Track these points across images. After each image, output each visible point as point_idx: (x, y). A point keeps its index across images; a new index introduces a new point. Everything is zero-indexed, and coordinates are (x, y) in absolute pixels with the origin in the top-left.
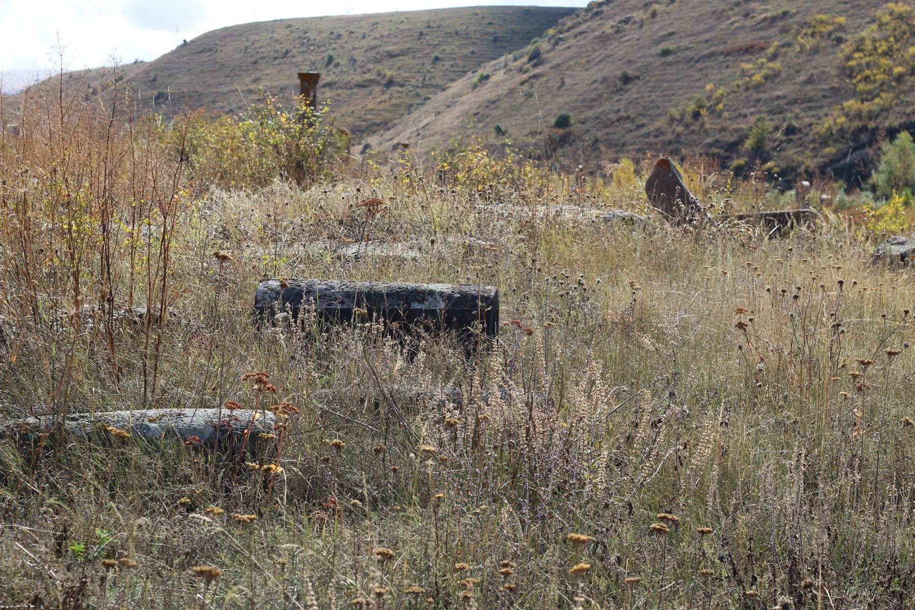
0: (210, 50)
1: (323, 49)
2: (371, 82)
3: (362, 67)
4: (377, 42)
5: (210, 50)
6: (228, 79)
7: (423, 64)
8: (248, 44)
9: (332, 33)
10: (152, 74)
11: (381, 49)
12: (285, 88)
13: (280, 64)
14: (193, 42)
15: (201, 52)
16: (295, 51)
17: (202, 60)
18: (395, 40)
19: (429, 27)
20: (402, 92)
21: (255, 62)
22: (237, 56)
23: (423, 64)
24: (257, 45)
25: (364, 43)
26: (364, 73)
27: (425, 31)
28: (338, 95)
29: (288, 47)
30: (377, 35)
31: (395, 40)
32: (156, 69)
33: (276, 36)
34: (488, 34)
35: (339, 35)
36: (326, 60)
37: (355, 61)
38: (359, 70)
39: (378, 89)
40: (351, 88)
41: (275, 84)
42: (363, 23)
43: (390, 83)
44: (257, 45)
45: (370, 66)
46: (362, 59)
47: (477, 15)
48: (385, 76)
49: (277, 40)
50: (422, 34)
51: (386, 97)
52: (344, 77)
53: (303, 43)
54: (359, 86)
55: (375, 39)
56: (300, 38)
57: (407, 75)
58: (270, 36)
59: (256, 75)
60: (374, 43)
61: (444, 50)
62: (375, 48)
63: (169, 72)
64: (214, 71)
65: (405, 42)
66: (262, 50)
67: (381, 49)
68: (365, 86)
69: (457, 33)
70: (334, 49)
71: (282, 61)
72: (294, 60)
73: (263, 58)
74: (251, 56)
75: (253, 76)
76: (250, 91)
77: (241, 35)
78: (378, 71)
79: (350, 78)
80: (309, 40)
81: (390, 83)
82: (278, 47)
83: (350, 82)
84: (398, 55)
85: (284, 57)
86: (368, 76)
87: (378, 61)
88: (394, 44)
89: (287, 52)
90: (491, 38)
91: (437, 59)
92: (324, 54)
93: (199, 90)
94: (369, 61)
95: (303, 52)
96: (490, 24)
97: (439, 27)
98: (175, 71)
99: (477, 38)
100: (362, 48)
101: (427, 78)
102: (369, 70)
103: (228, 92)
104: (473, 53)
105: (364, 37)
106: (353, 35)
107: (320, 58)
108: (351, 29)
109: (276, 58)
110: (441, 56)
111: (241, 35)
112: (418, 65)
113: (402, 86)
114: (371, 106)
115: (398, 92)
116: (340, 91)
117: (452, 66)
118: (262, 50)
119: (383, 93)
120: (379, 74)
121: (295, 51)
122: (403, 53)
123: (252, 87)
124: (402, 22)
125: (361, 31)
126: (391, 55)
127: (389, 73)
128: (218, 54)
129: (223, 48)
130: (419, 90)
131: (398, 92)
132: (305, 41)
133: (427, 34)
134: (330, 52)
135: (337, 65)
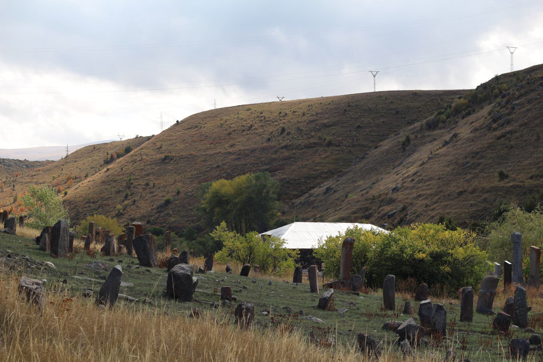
0: (196, 127)
1: (276, 123)
2: (315, 143)
3: (307, 134)
4: (315, 118)
5: (196, 127)
6: (212, 145)
7: (350, 131)
8: (222, 122)
9: (280, 113)
10: (159, 145)
11: (318, 122)
12: (255, 150)
13: (247, 134)
14: (183, 122)
15: (190, 128)
16: (256, 126)
17: (192, 133)
18: (327, 116)
19: (349, 106)
20: (339, 150)
21: (230, 134)
22: (216, 130)
23: (350, 131)
24: (228, 122)
25: (305, 118)
26: (309, 138)
27: (348, 109)
28: (293, 154)
29: (251, 123)
30: (313, 113)
31: (327, 116)
32: (161, 141)
33: (241, 116)
34: (391, 109)
35: (286, 114)
36: (280, 131)
37: (301, 130)
38: (305, 136)
39: (321, 149)
40: (302, 149)
41: (246, 148)
42: (301, 105)
43: (330, 144)
44: (228, 122)
45: (313, 134)
46: (306, 129)
47: (382, 97)
48: (325, 139)
49: (242, 119)
50: (345, 110)
51: (328, 154)
52: (296, 141)
53: (261, 120)
54: (306, 147)
55: (312, 115)
56: (258, 117)
57: (341, 139)
58: (237, 116)
59: (232, 142)
60: (312, 118)
61: (363, 121)
62: (314, 121)
63: (170, 142)
64: (201, 140)
65: (334, 117)
66: (233, 125)
67: (318, 122)
68: (313, 147)
69: (370, 110)
70: (284, 123)
71: (248, 132)
72: (257, 132)
73: (234, 130)
74: (226, 130)
75: (230, 143)
76: (230, 153)
77: (216, 116)
78: (320, 137)
79: (300, 142)
80: (265, 118)
81: (330, 144)
82: (244, 123)
83: (300, 145)
84: (332, 126)
85: (249, 130)
86: (312, 140)
87: (319, 130)
88: (327, 118)
89: (251, 126)
90: (394, 112)
91: (359, 127)
92: (278, 127)
93: (193, 153)
94: (311, 131)
95: (262, 126)
96: (392, 102)
97: (356, 105)
98: (174, 141)
99: (384, 113)
100: (305, 121)
101: (355, 140)
102: (313, 136)
103: (214, 154)
104: (383, 122)
105: (304, 115)
106: (296, 114)
107: (275, 129)
108: (293, 110)
109: (244, 131)
110: (362, 125)
111: (216, 116)
112: (346, 132)
113: (337, 146)
114: (318, 160)
115: (336, 150)
116: (294, 151)
117: (371, 131)
118: (233, 125)
119: (326, 151)
120: (320, 138)
121: (256, 126)
122: (334, 124)
123: (231, 150)
124: (330, 103)
125: (302, 111)
126: (326, 126)
127: (328, 138)
128: (202, 129)
129: (205, 125)
130: (351, 148)
131: (336, 150)
132: (262, 118)
133: (349, 111)
134: (281, 125)
135: (289, 134)
